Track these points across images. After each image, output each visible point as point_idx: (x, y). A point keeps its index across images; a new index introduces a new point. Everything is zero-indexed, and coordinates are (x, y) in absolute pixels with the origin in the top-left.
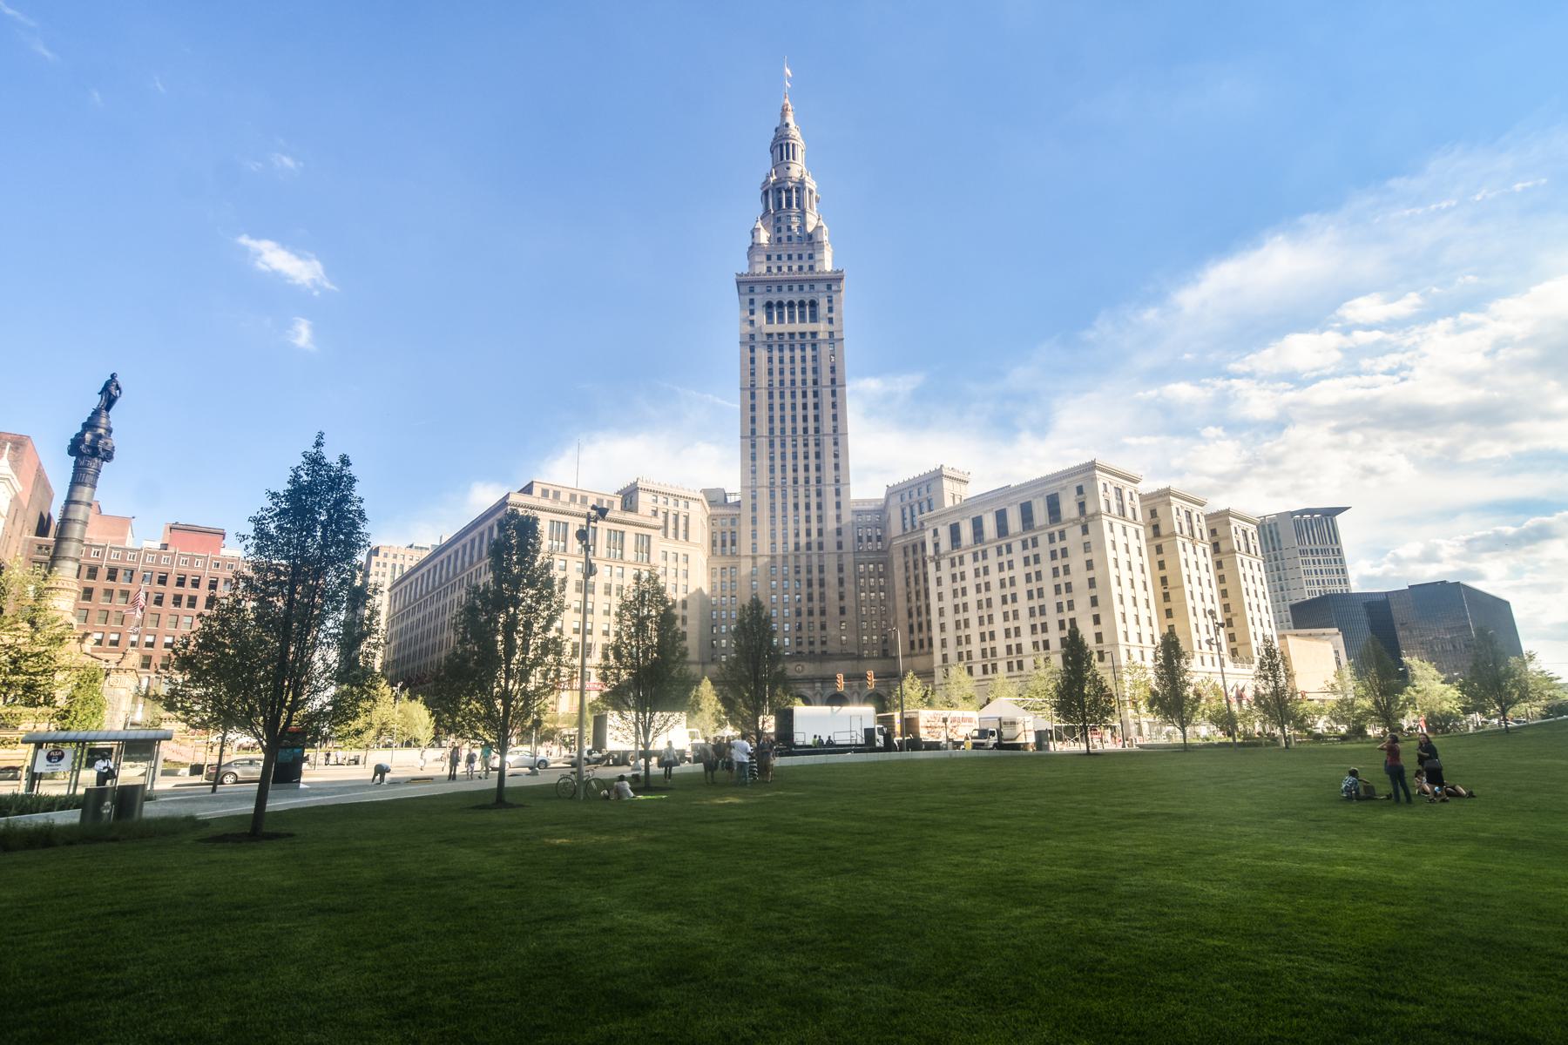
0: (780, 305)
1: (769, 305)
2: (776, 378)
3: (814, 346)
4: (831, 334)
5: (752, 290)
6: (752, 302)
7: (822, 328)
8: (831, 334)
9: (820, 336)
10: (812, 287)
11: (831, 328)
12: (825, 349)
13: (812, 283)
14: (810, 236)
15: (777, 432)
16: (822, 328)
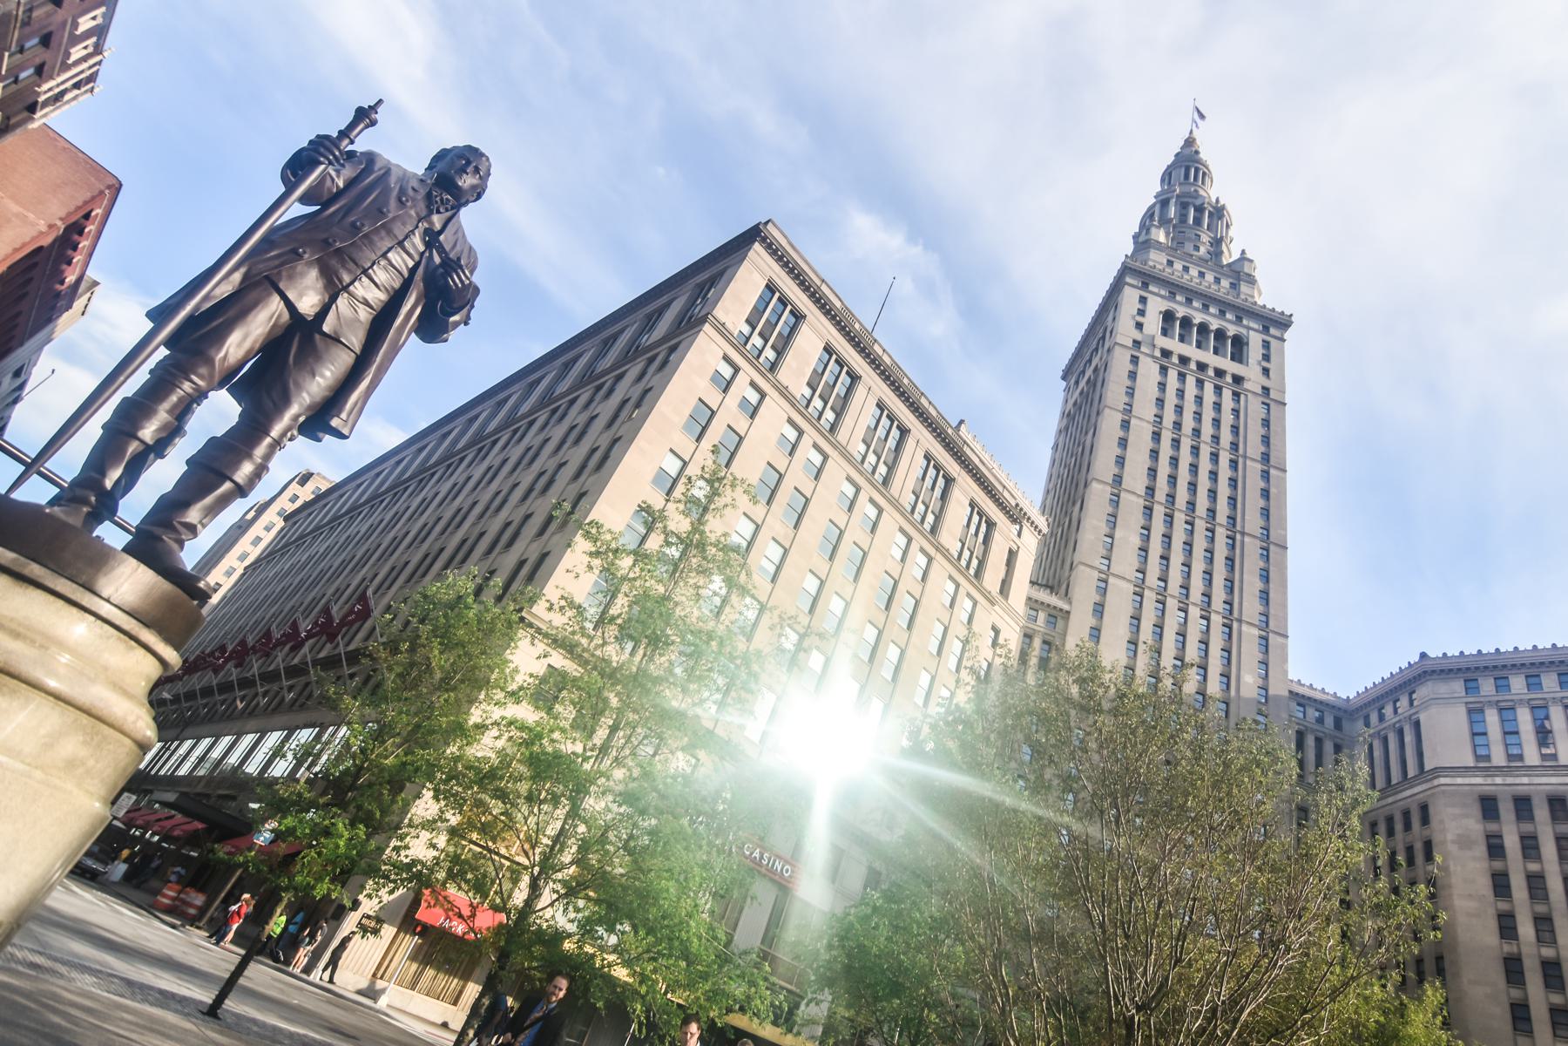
0: (1186, 322)
1: (1168, 317)
2: (1169, 417)
3: (1236, 395)
4: (1266, 390)
5: (1145, 286)
6: (1143, 300)
7: (1251, 371)
8: (1266, 390)
9: (1247, 385)
10: (1239, 319)
11: (1267, 383)
12: (1254, 409)
13: (1245, 312)
14: (1229, 265)
15: (1160, 495)
16: (1251, 371)
